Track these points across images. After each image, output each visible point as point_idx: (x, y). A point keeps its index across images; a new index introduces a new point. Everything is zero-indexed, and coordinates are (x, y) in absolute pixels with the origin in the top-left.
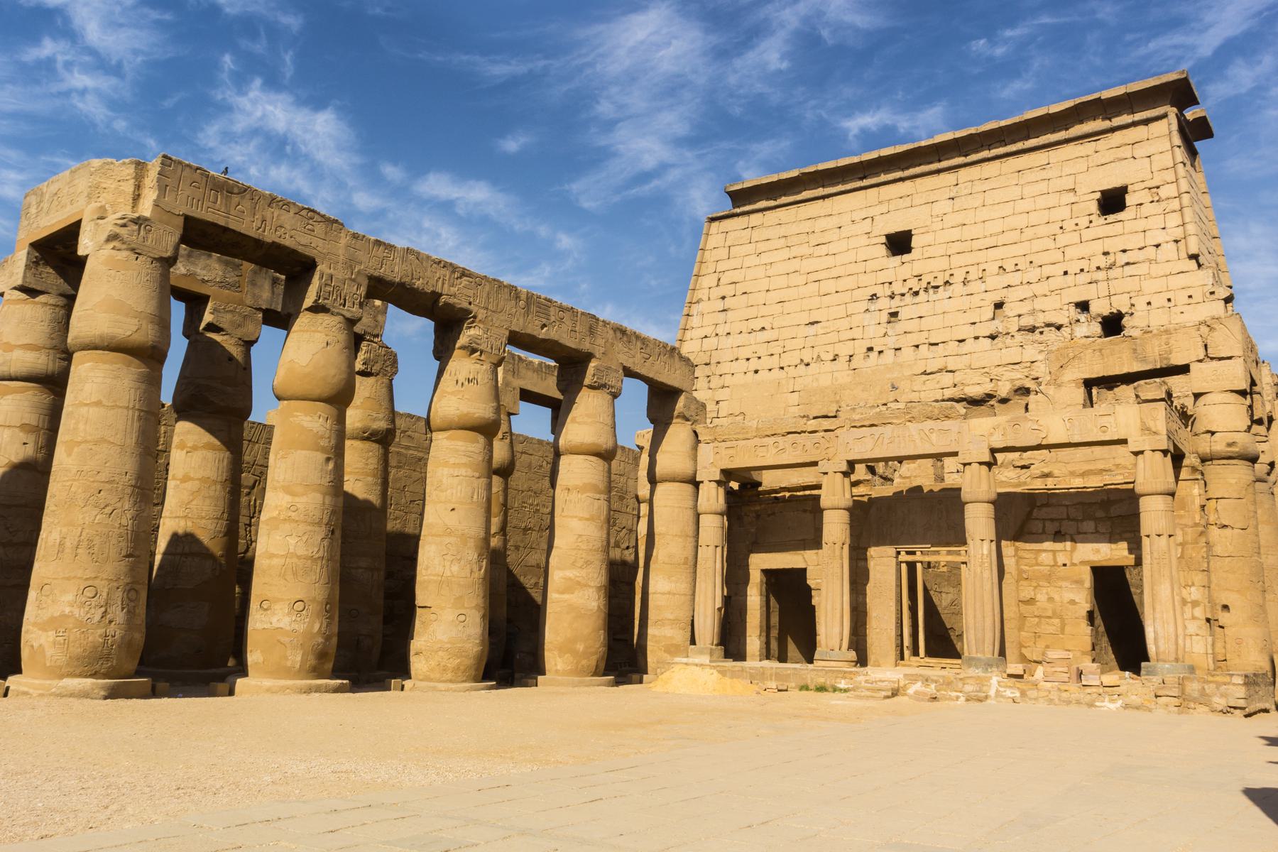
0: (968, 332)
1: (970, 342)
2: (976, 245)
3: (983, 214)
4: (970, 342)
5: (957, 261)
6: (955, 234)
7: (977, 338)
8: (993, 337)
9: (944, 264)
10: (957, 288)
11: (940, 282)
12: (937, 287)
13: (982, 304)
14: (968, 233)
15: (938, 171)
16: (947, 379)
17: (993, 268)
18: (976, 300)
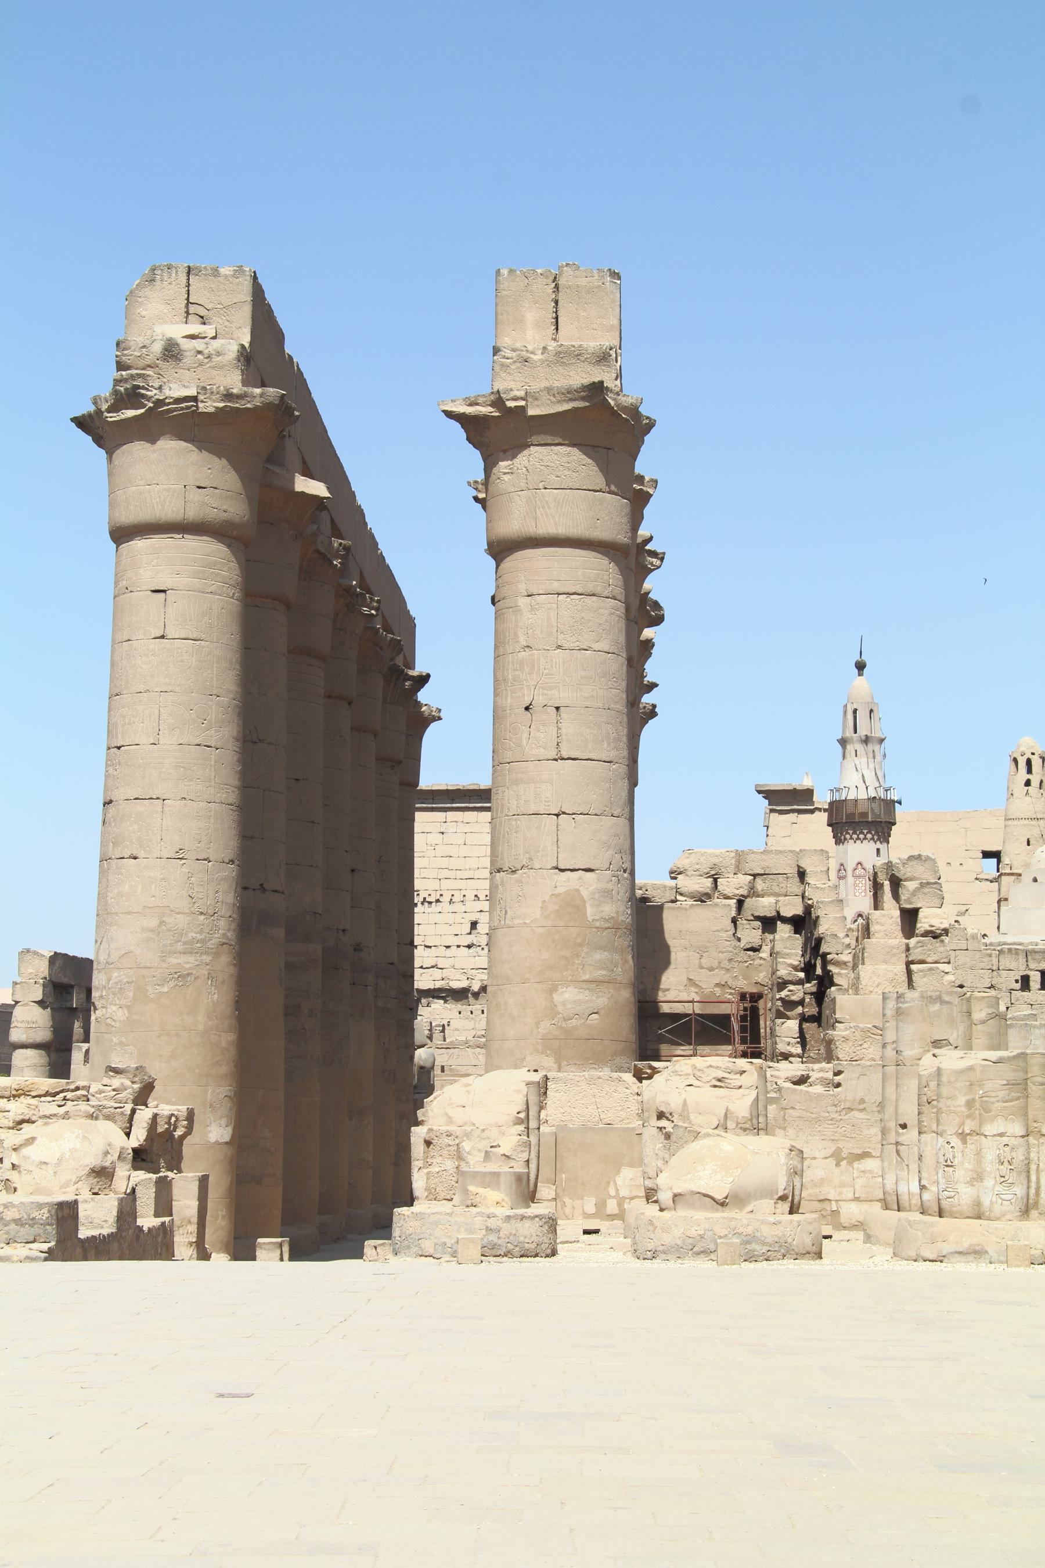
0: (453, 941)
1: (454, 948)
2: (459, 874)
3: (464, 851)
4: (454, 948)
5: (445, 884)
6: (444, 863)
7: (458, 946)
8: (469, 947)
9: (435, 884)
10: (444, 906)
11: (432, 899)
12: (430, 903)
13: (463, 921)
14: (454, 863)
15: (432, 810)
16: (437, 974)
17: (470, 896)
18: (458, 916)
